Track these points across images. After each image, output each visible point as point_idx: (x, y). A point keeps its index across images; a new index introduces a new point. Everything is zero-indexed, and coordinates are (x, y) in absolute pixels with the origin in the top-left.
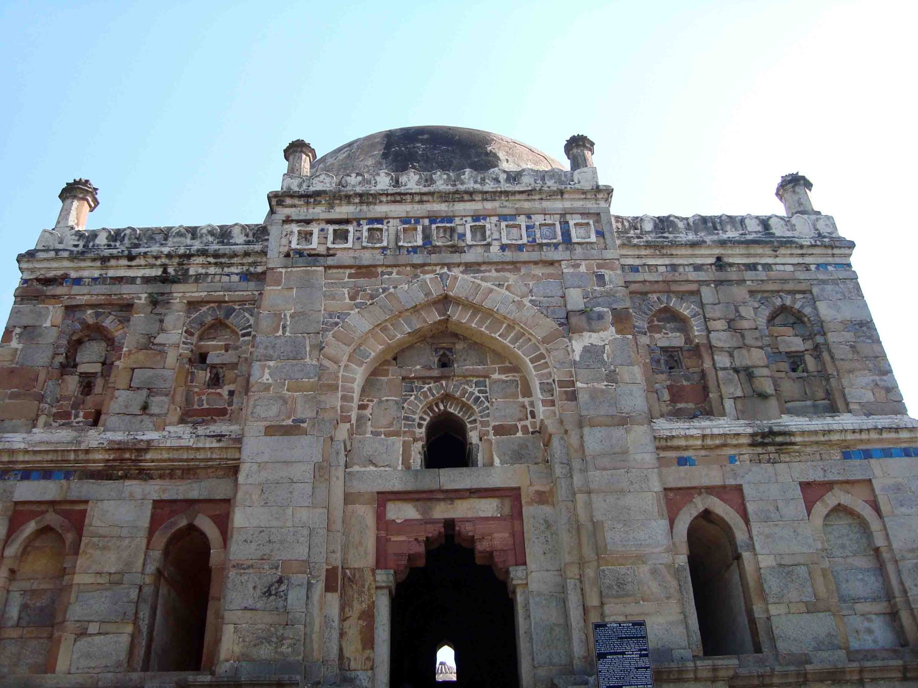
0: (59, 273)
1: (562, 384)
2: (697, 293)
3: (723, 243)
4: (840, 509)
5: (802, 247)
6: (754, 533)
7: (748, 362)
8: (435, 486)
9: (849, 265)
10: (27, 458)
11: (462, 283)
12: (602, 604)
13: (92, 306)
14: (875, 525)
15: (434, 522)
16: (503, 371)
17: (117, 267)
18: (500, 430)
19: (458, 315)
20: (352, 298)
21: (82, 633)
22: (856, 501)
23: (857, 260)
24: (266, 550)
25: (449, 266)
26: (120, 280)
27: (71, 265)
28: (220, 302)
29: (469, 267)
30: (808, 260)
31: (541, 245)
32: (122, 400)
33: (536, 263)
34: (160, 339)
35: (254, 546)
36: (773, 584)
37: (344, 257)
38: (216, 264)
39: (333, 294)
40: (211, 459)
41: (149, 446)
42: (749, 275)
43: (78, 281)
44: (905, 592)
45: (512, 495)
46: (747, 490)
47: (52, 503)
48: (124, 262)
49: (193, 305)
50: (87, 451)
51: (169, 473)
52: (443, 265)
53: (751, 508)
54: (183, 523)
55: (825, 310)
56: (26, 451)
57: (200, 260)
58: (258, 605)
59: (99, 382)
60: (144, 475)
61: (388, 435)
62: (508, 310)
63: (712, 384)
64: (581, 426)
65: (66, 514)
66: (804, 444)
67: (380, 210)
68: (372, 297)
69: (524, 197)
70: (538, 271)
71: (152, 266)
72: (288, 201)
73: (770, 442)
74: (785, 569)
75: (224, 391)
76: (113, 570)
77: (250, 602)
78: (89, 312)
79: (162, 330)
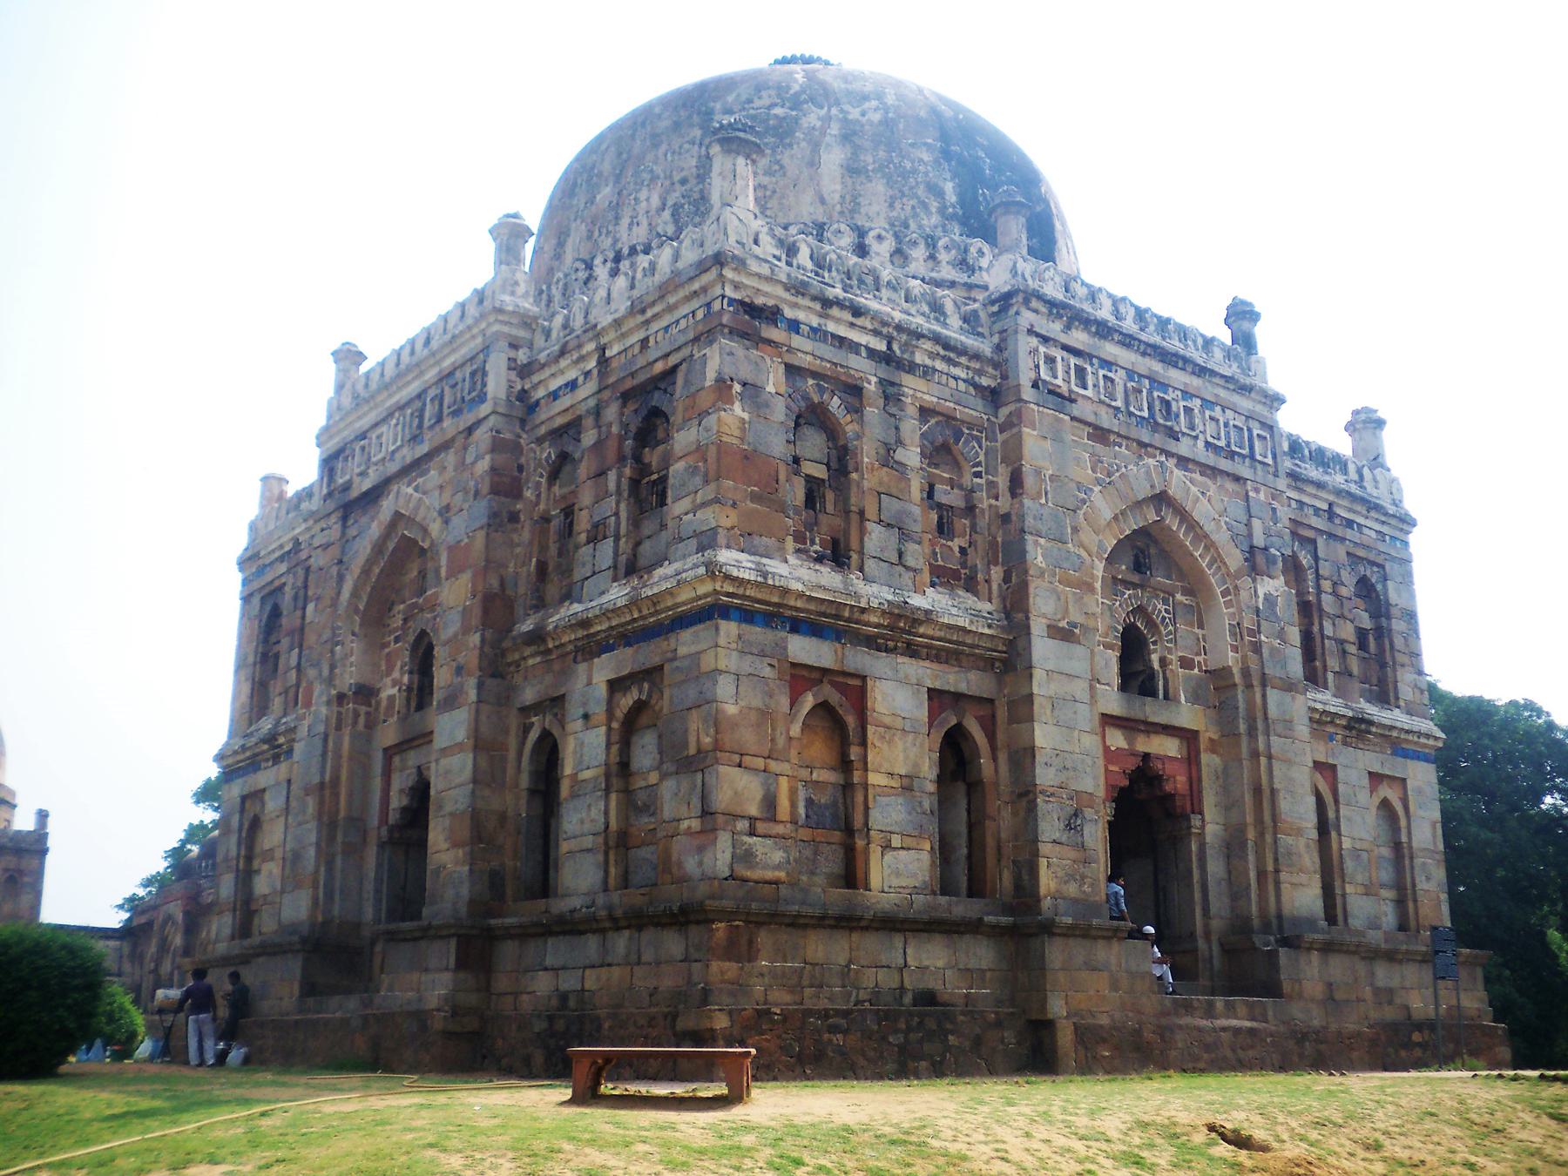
0: (771, 303)
1: (1251, 633)
2: (1314, 542)
3: (1339, 493)
4: (1385, 804)
5: (1386, 514)
6: (1342, 812)
7: (1343, 636)
8: (1140, 716)
9: (1406, 544)
10: (799, 604)
11: (1179, 482)
12: (1277, 871)
13: (815, 375)
14: (1403, 823)
15: (1134, 754)
16: (1186, 592)
17: (838, 321)
18: (1186, 663)
19: (1172, 522)
20: (1094, 471)
21: (887, 847)
22: (1392, 795)
23: (1415, 539)
24: (1063, 777)
25: (1169, 454)
26: (841, 342)
27: (787, 296)
28: (949, 418)
29: (1183, 462)
30: (1385, 529)
31: (1234, 453)
32: (876, 538)
33: (1228, 474)
34: (900, 455)
35: (1052, 770)
36: (1349, 864)
37: (1082, 409)
38: (943, 358)
39: (1080, 460)
40: (978, 646)
41: (928, 616)
42: (1349, 534)
43: (794, 326)
44: (1414, 885)
45: (1188, 737)
46: (1341, 774)
47: (825, 671)
48: (847, 316)
49: (925, 412)
50: (863, 610)
51: (939, 656)
52: (1163, 451)
53: (1341, 788)
54: (954, 721)
55: (1393, 597)
56: (801, 595)
57: (928, 345)
58: (1064, 839)
59: (830, 496)
60: (912, 651)
61: (1107, 646)
62: (1209, 527)
63: (1319, 650)
64: (1264, 685)
65: (843, 689)
66: (1375, 734)
67: (1110, 350)
68: (1109, 475)
69: (1221, 382)
70: (1230, 486)
71: (876, 333)
72: (1034, 304)
73: (1358, 728)
74: (1356, 852)
75: (955, 544)
76: (903, 772)
77: (1056, 836)
78: (811, 382)
79: (900, 442)
